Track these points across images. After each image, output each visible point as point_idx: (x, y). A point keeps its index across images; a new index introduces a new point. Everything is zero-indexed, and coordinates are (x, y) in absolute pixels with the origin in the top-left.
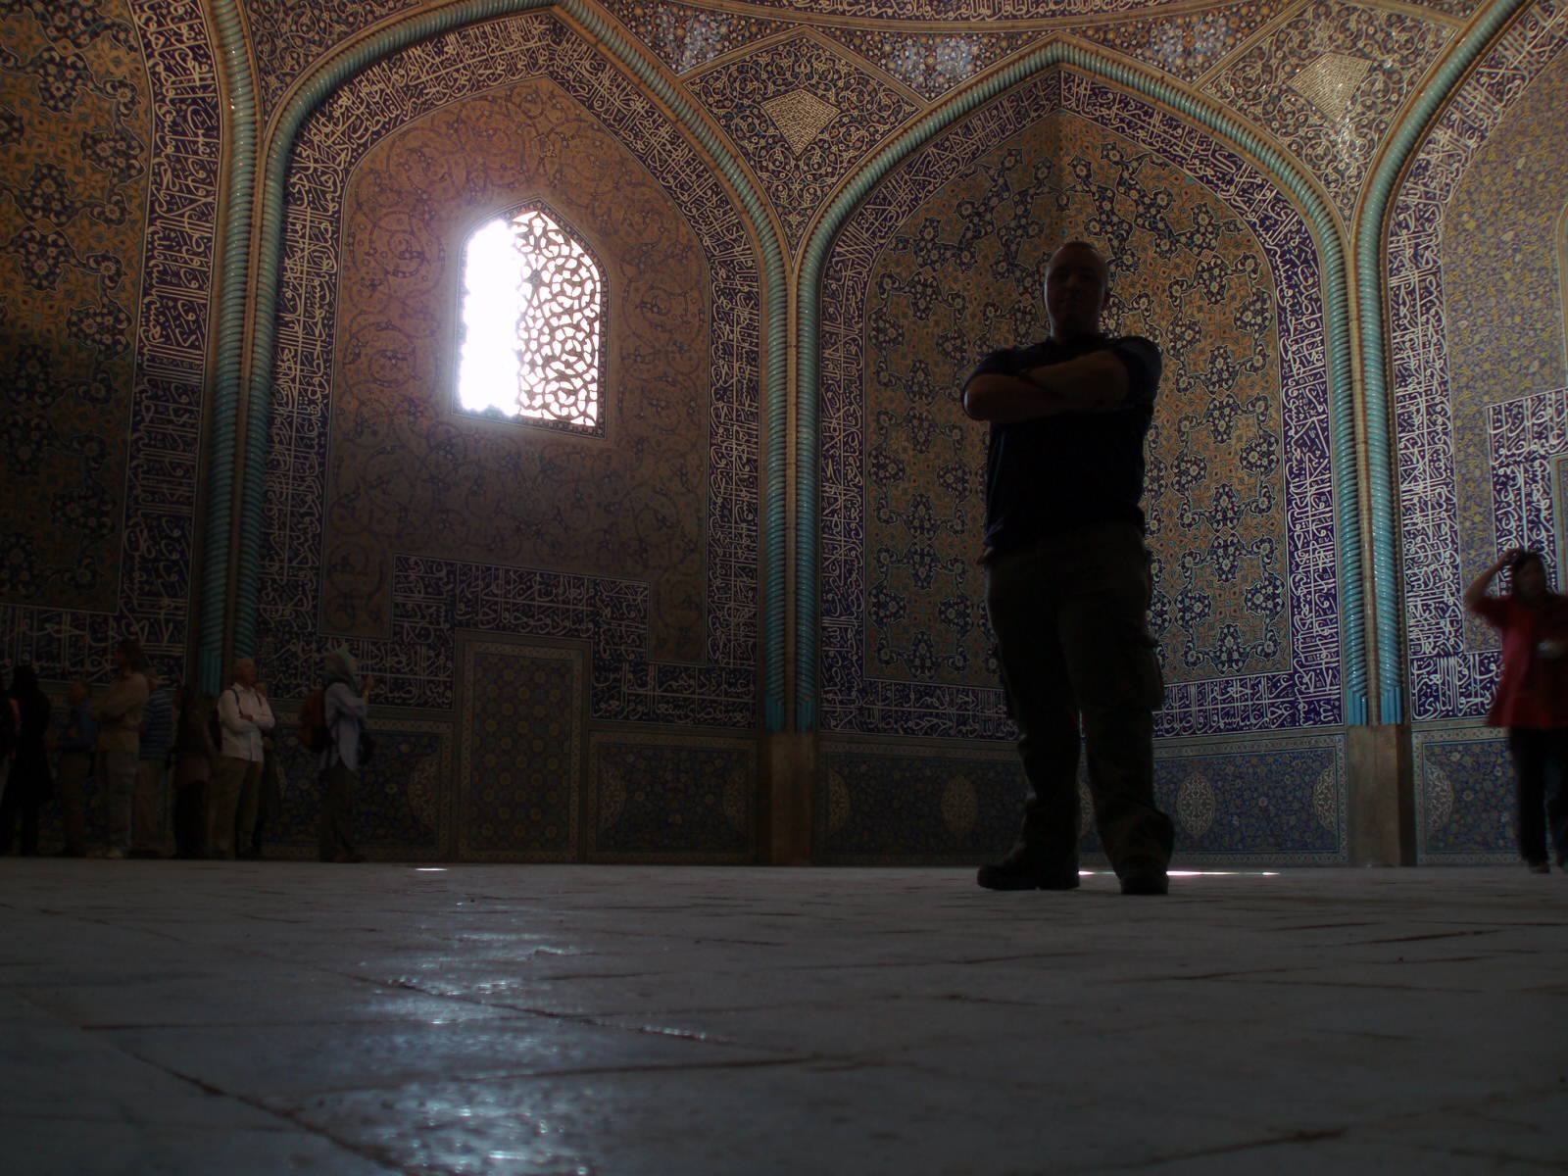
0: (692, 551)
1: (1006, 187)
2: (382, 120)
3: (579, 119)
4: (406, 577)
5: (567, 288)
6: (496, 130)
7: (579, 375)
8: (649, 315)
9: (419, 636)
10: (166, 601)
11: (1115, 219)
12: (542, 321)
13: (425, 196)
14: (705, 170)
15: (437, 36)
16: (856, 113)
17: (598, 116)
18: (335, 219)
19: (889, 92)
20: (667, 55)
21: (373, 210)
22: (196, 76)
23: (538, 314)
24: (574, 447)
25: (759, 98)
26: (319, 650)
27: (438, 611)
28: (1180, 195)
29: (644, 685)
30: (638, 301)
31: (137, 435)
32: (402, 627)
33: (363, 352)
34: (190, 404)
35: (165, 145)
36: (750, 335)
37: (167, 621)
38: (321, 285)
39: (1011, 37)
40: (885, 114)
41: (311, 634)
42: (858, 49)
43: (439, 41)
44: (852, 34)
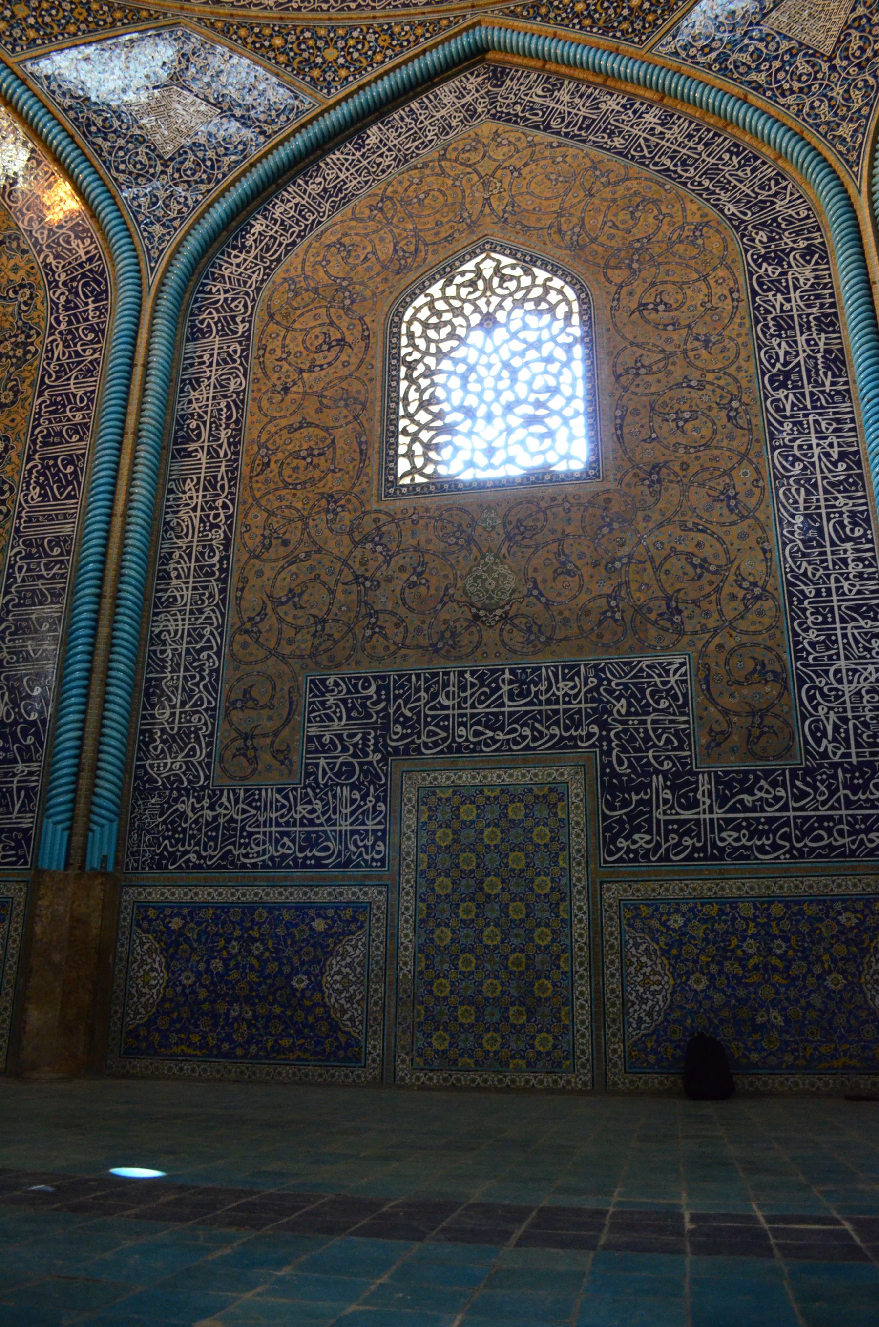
0: (758, 598)
2: (297, 229)
3: (532, 145)
4: (323, 703)
5: (532, 320)
6: (427, 193)
8: (653, 316)
9: (338, 775)
10: (20, 767)
14: (716, 134)
17: (558, 133)
18: (247, 336)
20: (624, 32)
21: (286, 316)
22: (81, 252)
23: (494, 359)
24: (553, 499)
26: (212, 808)
27: (365, 739)
29: (693, 804)
30: (634, 305)
31: (8, 597)
32: (317, 765)
33: (273, 459)
34: (61, 554)
35: (58, 323)
36: (818, 297)
37: (19, 789)
38: (228, 406)
41: (203, 788)
43: (360, 137)
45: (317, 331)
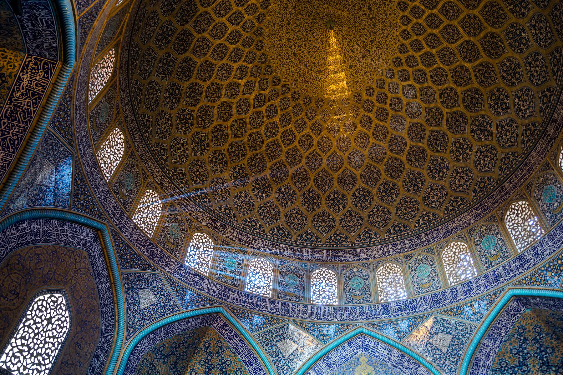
1: (186, 342)
2: (33, 238)
3: (88, 269)
5: (58, 327)
7: (45, 365)
8: (77, 348)
11: (210, 363)
12: (43, 338)
13: (31, 273)
15: (63, 221)
16: (162, 304)
19: (174, 302)
21: (11, 269)
25: (139, 287)
28: (234, 363)
36: (101, 367)
39: (210, 300)
40: (170, 308)
42: (171, 285)
44: (171, 280)
45: (15, 284)
